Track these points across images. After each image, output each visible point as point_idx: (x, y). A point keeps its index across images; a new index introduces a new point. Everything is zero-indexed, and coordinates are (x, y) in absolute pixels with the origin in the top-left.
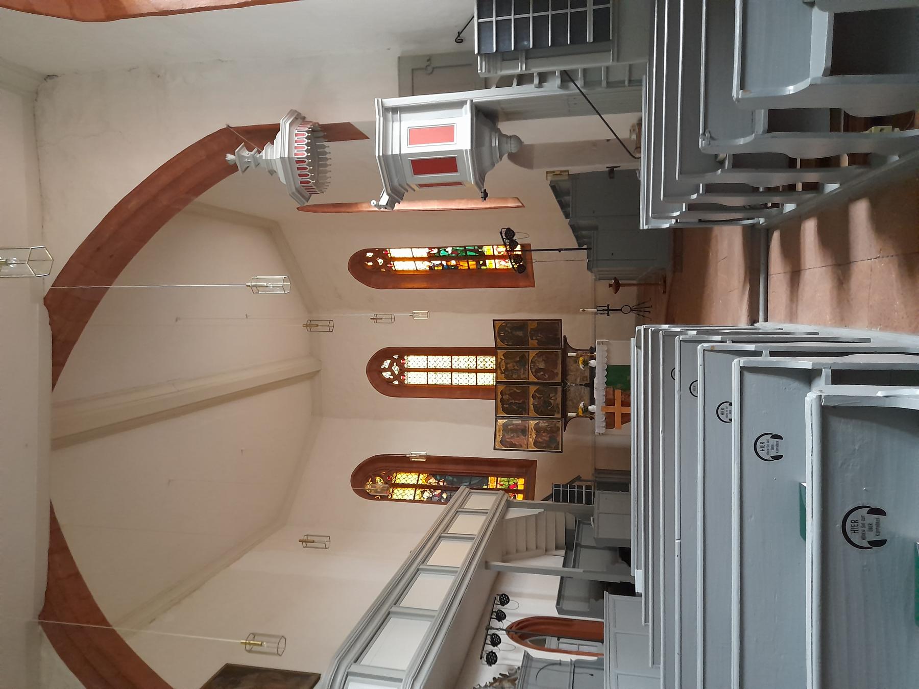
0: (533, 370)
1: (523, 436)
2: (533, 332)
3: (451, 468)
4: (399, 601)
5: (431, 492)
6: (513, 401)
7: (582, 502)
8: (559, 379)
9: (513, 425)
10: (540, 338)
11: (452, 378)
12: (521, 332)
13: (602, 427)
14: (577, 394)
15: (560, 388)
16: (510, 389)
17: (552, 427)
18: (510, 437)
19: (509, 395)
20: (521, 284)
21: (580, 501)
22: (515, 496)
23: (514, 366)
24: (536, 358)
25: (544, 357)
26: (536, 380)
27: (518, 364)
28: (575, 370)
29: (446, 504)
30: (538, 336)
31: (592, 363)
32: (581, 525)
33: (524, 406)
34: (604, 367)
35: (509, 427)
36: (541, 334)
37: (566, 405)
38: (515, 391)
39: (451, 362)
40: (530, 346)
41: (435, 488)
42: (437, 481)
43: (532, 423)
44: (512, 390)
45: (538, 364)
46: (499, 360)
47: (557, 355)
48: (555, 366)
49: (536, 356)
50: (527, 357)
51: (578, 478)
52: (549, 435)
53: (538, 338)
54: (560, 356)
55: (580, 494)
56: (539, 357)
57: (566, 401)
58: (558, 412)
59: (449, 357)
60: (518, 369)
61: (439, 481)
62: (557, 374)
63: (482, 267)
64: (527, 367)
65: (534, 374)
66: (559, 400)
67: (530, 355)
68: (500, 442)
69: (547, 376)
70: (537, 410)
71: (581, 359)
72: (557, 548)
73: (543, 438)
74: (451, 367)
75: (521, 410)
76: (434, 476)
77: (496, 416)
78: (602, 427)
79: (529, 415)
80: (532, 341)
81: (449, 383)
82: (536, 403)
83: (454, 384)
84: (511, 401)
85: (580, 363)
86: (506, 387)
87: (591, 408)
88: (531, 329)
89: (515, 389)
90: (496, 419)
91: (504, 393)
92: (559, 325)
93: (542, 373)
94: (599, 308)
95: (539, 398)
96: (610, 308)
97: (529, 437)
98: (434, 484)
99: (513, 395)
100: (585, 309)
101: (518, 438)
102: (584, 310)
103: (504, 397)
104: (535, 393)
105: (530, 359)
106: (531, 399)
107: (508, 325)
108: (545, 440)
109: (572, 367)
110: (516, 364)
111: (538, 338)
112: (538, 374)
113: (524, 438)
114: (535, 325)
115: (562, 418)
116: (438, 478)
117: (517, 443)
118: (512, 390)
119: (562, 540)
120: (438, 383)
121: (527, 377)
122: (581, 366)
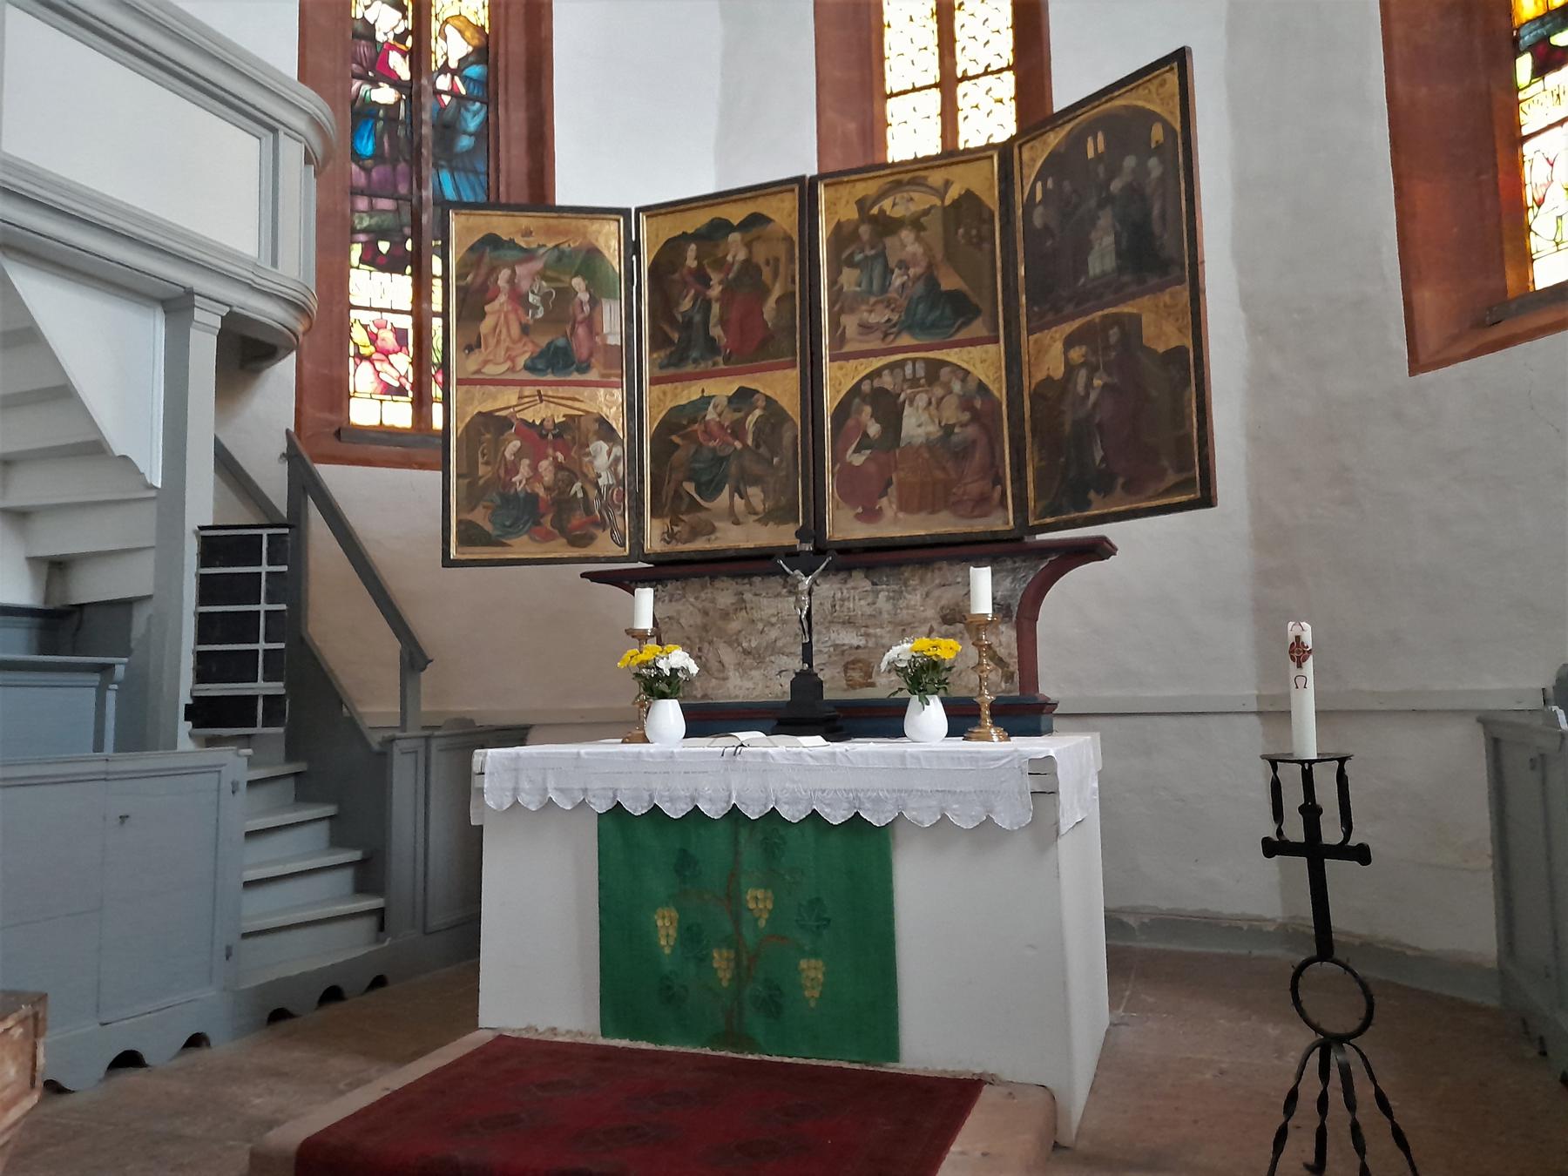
0: (887, 381)
1: (532, 359)
2: (1114, 334)
3: (514, 121)
4: (241, 117)
5: (400, 38)
6: (715, 291)
7: (201, 676)
8: (843, 525)
9: (594, 302)
10: (1080, 388)
11: (914, 90)
12: (1110, 263)
13: (516, 791)
14: (773, 633)
15: (783, 536)
16: (777, 260)
17: (588, 510)
18: (524, 285)
19: (747, 262)
20: (1427, 297)
21: (207, 668)
22: (401, 391)
23: (904, 265)
24: (957, 387)
25: (972, 431)
26: (829, 403)
27: (920, 288)
28: (904, 615)
29: (302, 77)
30: (1089, 385)
31: (929, 718)
32: (96, 678)
33: (695, 354)
34: (877, 801)
35: (578, 283)
36: (1105, 386)
37: (713, 578)
38: (765, 292)
39: (986, 73)
40: (1027, 342)
41: (418, 56)
42: (453, 64)
43: (609, 403)
44: (776, 275)
45: (922, 400)
46: (936, 178)
47: (982, 504)
48: (919, 500)
49: (972, 385)
50: (960, 336)
51: (414, 659)
52: (541, 492)
53: (1082, 376)
54: (979, 526)
55: (243, 667)
56: (966, 404)
57: (734, 576)
58: (670, 536)
59: (1008, 57)
60: (892, 294)
61: (454, 73)
62: (871, 514)
63: (1524, 64)
64: (906, 340)
65: (866, 387)
66: (733, 537)
67: (976, 351)
68: (492, 241)
69: (858, 460)
70: (676, 424)
71: (947, 649)
72: (56, 568)
73: (526, 462)
74: (965, 78)
75: (675, 336)
76: (484, 52)
77: (638, 210)
78: (516, 791)
79: (654, 382)
80: (1058, 347)
81: (893, 82)
82: (711, 415)
83: (891, 103)
84: (715, 278)
85: (923, 643)
86: (788, 239)
87: (668, 716)
88: (1136, 319)
89: (777, 292)
90: (625, 212)
91: (754, 232)
92: (1168, 492)
93: (874, 429)
94: (1325, 779)
95: (737, 430)
96: (1330, 865)
97: (528, 390)
98: (439, 53)
99: (749, 280)
100: (1309, 665)
101: (515, 330)
102: (1298, 652)
103: (735, 237)
104: (762, 403)
105: (952, 356)
106: (722, 389)
107: (1153, 162)
108: (513, 469)
109: (915, 598)
110: (917, 278)
111: (1082, 376)
112: (868, 409)
113: (521, 362)
114: (1162, 334)
115: (645, 558)
116: (475, 71)
117: (486, 326)
118: (776, 275)
119: (90, 588)
120: (889, 36)
121: (846, 349)
122: (902, 651)
